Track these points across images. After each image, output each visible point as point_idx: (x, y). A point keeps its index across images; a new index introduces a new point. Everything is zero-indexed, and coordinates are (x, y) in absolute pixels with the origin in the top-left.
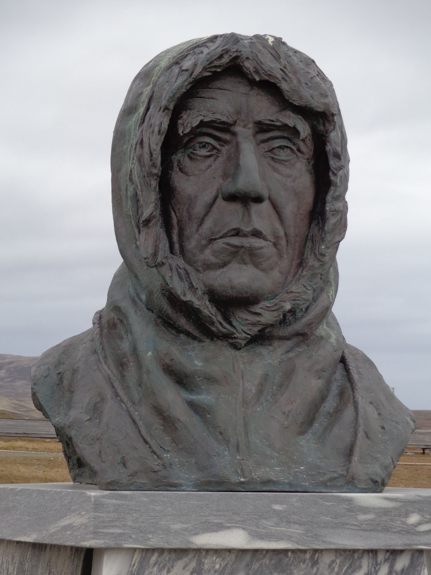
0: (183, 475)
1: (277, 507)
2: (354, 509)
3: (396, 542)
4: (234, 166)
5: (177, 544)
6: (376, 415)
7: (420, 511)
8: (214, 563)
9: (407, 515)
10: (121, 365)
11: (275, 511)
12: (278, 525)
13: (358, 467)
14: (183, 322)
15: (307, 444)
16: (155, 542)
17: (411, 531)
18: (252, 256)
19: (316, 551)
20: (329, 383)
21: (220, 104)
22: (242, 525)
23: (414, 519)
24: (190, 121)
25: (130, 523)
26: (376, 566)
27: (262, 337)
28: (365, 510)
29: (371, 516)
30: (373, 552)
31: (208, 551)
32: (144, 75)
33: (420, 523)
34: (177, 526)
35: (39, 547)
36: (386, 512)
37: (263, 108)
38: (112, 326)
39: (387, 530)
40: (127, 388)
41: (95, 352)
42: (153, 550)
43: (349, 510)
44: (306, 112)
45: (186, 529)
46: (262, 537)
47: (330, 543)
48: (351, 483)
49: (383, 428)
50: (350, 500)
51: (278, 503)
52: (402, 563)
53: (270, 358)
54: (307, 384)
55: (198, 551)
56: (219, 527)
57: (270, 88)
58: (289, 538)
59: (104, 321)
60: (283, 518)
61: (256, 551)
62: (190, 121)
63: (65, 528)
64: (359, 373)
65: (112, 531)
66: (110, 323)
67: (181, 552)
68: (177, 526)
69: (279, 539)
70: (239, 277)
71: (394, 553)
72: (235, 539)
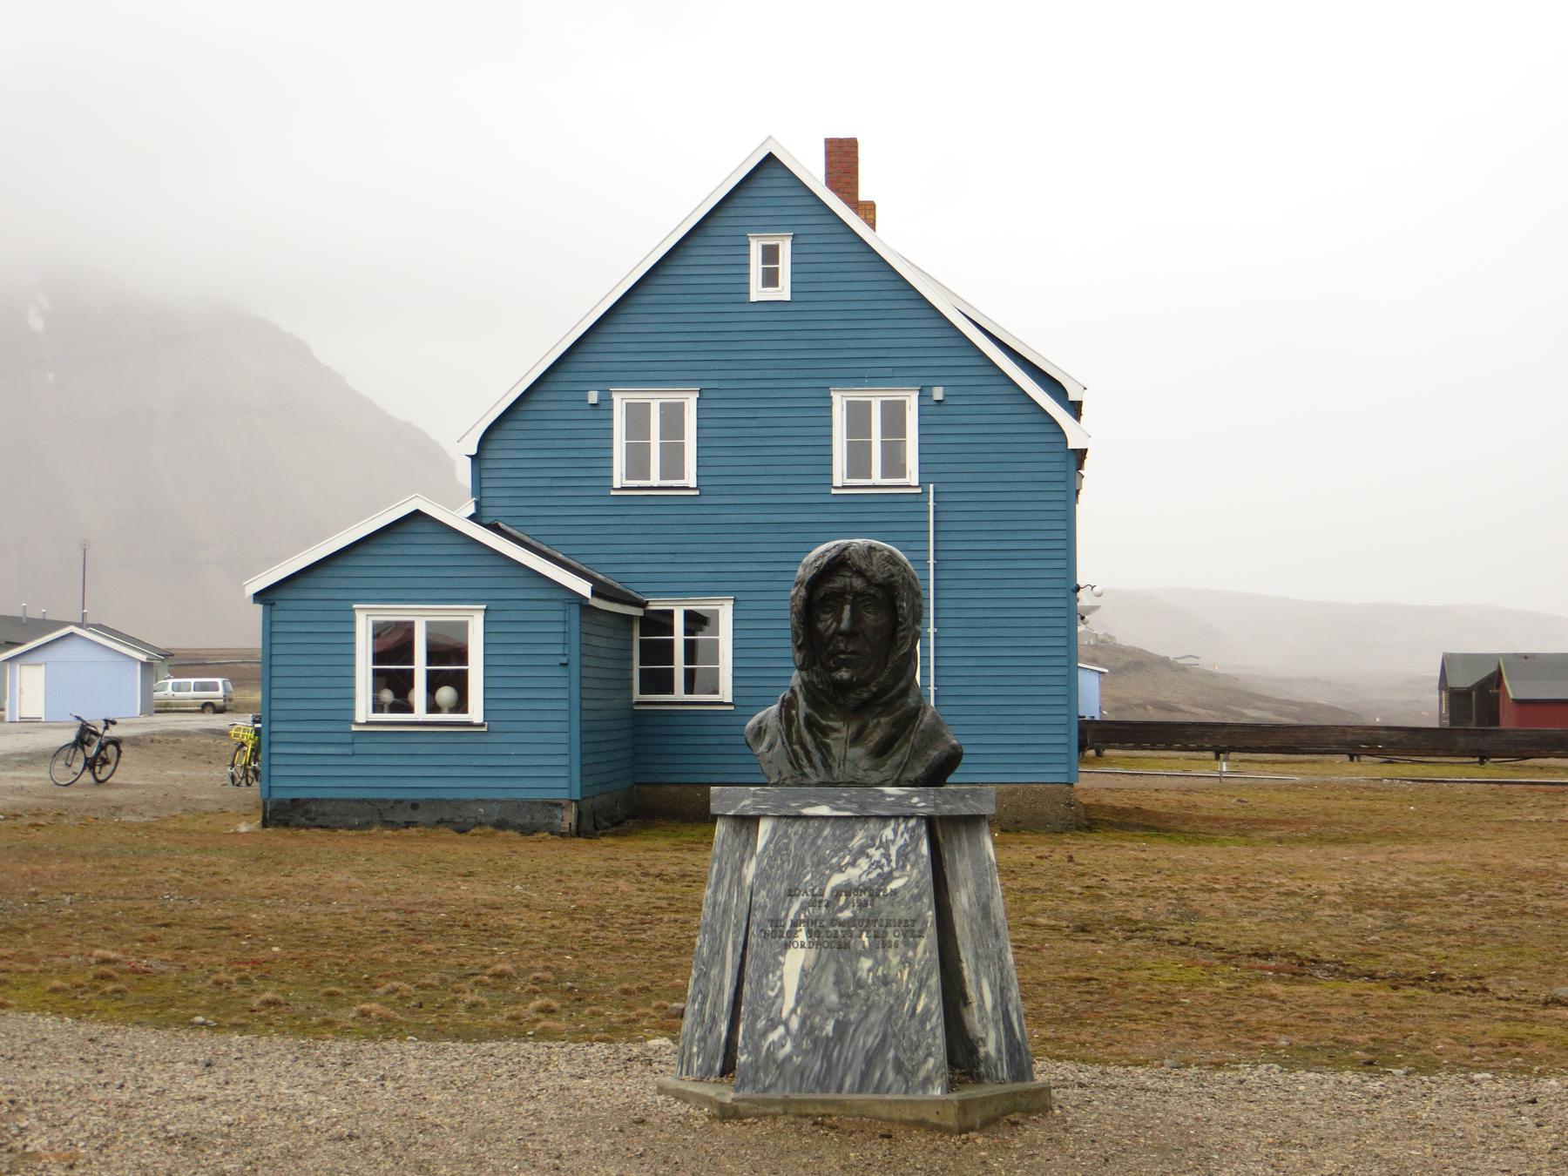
2: (884, 795)
3: (908, 812)
17: (914, 806)
22: (827, 803)
23: (915, 800)
30: (896, 817)
52: (912, 823)
60: (849, 801)
61: (837, 817)
72: (824, 810)
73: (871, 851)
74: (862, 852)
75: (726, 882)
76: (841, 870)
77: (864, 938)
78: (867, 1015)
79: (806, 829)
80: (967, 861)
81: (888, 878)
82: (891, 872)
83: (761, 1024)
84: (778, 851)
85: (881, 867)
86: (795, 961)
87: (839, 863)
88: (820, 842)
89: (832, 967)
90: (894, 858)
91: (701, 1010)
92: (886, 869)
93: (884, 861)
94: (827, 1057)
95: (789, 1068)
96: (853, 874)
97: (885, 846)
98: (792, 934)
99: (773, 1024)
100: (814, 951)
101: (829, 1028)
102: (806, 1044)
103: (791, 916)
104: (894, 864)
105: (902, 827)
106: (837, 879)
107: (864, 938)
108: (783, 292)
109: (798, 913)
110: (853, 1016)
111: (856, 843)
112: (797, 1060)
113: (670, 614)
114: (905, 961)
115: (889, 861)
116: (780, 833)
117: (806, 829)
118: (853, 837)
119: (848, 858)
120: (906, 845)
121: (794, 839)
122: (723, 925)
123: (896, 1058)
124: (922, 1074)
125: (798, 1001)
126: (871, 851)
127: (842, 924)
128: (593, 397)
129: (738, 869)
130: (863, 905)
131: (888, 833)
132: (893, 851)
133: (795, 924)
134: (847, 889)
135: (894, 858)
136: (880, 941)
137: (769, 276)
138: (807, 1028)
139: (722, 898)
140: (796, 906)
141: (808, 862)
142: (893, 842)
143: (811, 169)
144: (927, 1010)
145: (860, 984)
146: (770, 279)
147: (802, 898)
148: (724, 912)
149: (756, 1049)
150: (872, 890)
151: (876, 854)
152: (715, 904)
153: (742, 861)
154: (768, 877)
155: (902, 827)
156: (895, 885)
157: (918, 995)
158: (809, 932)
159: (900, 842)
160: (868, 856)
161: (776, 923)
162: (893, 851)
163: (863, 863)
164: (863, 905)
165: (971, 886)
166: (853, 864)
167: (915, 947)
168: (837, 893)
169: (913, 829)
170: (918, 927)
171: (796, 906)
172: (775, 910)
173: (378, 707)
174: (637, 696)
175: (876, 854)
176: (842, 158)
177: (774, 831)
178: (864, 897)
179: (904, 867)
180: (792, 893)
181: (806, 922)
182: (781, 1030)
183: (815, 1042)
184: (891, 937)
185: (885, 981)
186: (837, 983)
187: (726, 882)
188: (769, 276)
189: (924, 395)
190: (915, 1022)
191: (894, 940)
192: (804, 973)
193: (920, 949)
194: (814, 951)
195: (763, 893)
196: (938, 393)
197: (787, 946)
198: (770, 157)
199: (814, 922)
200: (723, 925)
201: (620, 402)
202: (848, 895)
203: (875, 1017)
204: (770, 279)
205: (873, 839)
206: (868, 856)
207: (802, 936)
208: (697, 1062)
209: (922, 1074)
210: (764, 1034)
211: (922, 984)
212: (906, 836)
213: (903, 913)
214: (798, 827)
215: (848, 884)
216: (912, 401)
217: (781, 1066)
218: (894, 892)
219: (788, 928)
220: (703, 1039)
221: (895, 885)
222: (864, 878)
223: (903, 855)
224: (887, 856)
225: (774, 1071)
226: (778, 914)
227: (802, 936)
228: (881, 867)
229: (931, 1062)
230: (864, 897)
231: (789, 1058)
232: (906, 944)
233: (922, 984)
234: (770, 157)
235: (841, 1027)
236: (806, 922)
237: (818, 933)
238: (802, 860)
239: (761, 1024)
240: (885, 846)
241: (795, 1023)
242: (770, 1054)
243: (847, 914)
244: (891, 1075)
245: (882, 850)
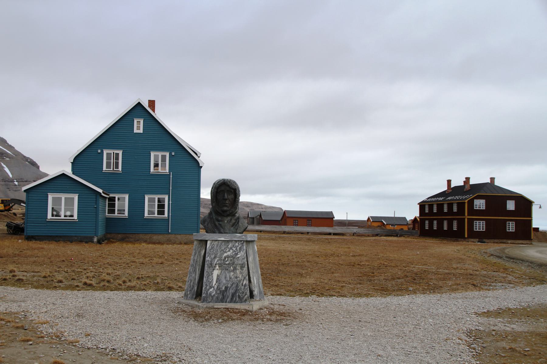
0: (217, 232)
4: (224, 196)
10: (211, 219)
13: (238, 231)
15: (232, 228)
18: (226, 206)
21: (223, 188)
24: (219, 190)
27: (228, 216)
32: (214, 184)
35: (201, 240)
37: (228, 188)
44: (233, 189)
48: (236, 233)
51: (228, 235)
53: (229, 218)
54: (233, 221)
57: (228, 186)
62: (219, 190)
66: (210, 214)
70: (225, 208)
71: (241, 241)
72: (223, 239)
74: (231, 248)
76: (226, 252)
78: (232, 285)
81: (237, 254)
83: (208, 287)
84: (212, 248)
86: (216, 273)
89: (224, 274)
91: (190, 284)
94: (223, 295)
95: (215, 298)
96: (229, 253)
97: (236, 247)
98: (215, 267)
99: (211, 287)
100: (220, 271)
101: (224, 288)
102: (218, 292)
106: (225, 254)
108: (141, 131)
110: (229, 285)
111: (229, 246)
112: (216, 295)
113: (115, 197)
114: (241, 273)
123: (239, 295)
124: (244, 299)
125: (217, 282)
128: (99, 151)
129: (200, 252)
130: (231, 260)
131: (237, 244)
132: (238, 248)
133: (216, 264)
134: (228, 257)
136: (235, 269)
138: (218, 288)
139: (196, 258)
140: (216, 261)
143: (146, 105)
144: (245, 284)
145: (230, 278)
146: (138, 128)
149: (207, 293)
150: (233, 257)
151: (234, 249)
152: (194, 260)
156: (238, 256)
157: (243, 281)
161: (211, 264)
162: (238, 248)
163: (231, 251)
164: (231, 260)
166: (229, 251)
168: (225, 258)
171: (216, 261)
172: (211, 261)
173: (53, 215)
174: (107, 214)
175: (234, 249)
176: (152, 104)
177: (211, 243)
180: (215, 258)
182: (213, 289)
183: (220, 291)
184: (237, 268)
185: (236, 278)
186: (225, 278)
189: (170, 154)
190: (243, 287)
192: (218, 276)
196: (173, 154)
197: (214, 269)
198: (139, 103)
201: (105, 152)
203: (234, 286)
204: (138, 128)
207: (217, 267)
208: (189, 296)
209: (244, 299)
210: (209, 290)
211: (245, 278)
213: (240, 262)
214: (216, 242)
216: (167, 154)
217: (213, 297)
220: (191, 291)
221: (238, 256)
223: (240, 249)
224: (236, 249)
225: (211, 298)
227: (217, 267)
229: (246, 296)
231: (214, 295)
233: (245, 278)
235: (226, 288)
239: (208, 287)
240: (236, 247)
241: (216, 287)
242: (210, 294)
243: (227, 262)
244: (238, 299)
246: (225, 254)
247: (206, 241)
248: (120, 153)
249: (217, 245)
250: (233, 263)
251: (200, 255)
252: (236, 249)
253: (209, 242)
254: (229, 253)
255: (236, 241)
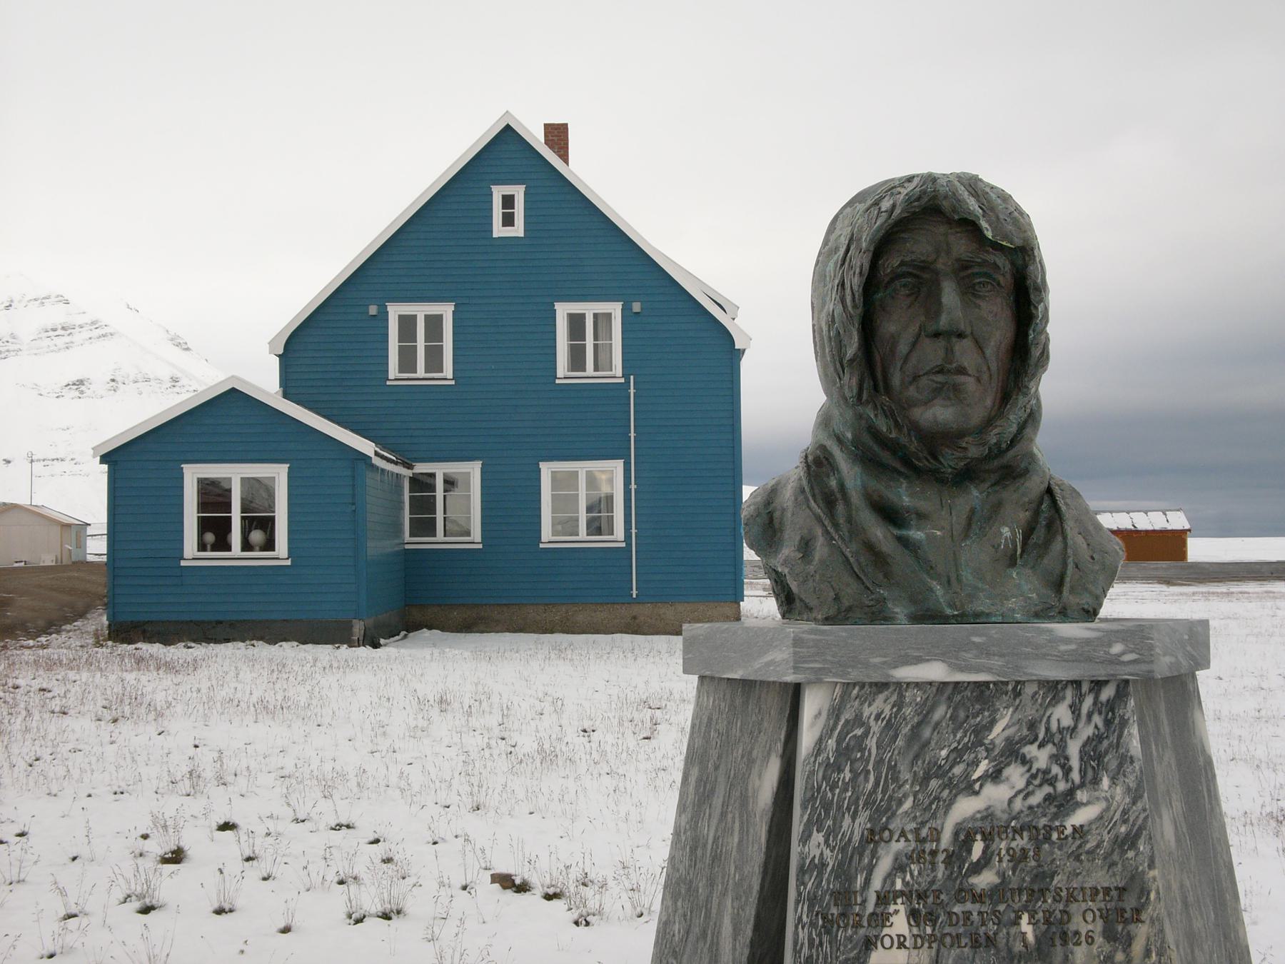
1: (976, 639)
2: (1057, 640)
3: (1101, 673)
5: (877, 677)
6: (1085, 546)
7: (1124, 640)
8: (915, 695)
9: (1110, 646)
11: (974, 643)
12: (977, 657)
14: (886, 457)
16: (854, 675)
17: (1115, 661)
19: (1018, 682)
20: (1037, 512)
23: (1117, 648)
25: (829, 658)
26: (1081, 698)
28: (1068, 641)
29: (1073, 647)
30: (1077, 684)
31: (908, 684)
33: (1123, 653)
34: (877, 660)
35: (747, 686)
36: (1088, 642)
38: (818, 462)
39: (1089, 659)
40: (836, 526)
41: (803, 491)
42: (855, 685)
43: (1050, 641)
45: (884, 663)
46: (961, 669)
47: (1032, 675)
49: (1092, 558)
50: (1050, 631)
55: (899, 684)
56: (918, 660)
58: (989, 670)
59: (810, 458)
60: (983, 650)
61: (957, 684)
63: (768, 664)
64: (1066, 504)
65: (811, 665)
67: (881, 686)
68: (877, 660)
69: (978, 670)
71: (1098, 685)
72: (935, 671)
73: (1031, 750)
74: (1012, 752)
75: (718, 801)
76: (970, 789)
77: (1026, 926)
79: (899, 705)
80: (1169, 756)
81: (1065, 803)
82: (1071, 792)
84: (844, 753)
85: (1052, 782)
87: (967, 774)
88: (927, 733)
90: (1075, 763)
92: (1062, 786)
93: (1056, 770)
96: (995, 795)
98: (881, 919)
103: (877, 884)
104: (1075, 776)
105: (1088, 702)
106: (966, 807)
107: (1026, 926)
109: (890, 877)
111: (998, 733)
115: (1067, 771)
116: (847, 715)
117: (899, 705)
118: (993, 722)
119: (984, 766)
120: (1098, 738)
121: (876, 728)
122: (711, 883)
126: (1031, 750)
127: (978, 898)
128: (373, 310)
130: (1018, 858)
131: (1061, 714)
132: (1074, 749)
134: (988, 827)
135: (1075, 763)
137: (508, 217)
140: (885, 864)
141: (906, 775)
142: (1073, 730)
143: (536, 137)
147: (898, 846)
148: (716, 858)
150: (1039, 826)
151: (1041, 757)
153: (751, 762)
154: (827, 806)
155: (1088, 702)
156: (1081, 817)
158: (913, 915)
159: (1086, 732)
160: (1024, 761)
161: (844, 896)
162: (1074, 749)
163: (1016, 775)
165: (1178, 805)
166: (995, 776)
167: (1128, 941)
168: (964, 838)
169: (1111, 706)
170: (1130, 903)
171: (885, 864)
172: (844, 872)
173: (202, 547)
174: (407, 538)
175: (1041, 757)
178: (1021, 842)
179: (1096, 781)
180: (874, 837)
181: (906, 895)
187: (718, 801)
188: (508, 217)
191: (1083, 929)
193: (1138, 948)
194: (925, 955)
195: (818, 837)
199: (922, 896)
200: (711, 883)
201: (395, 311)
202: (987, 838)
205: (1032, 726)
206: (1024, 761)
207: (899, 924)
212: (1097, 719)
213: (1100, 878)
215: (988, 814)
218: (1079, 831)
219: (870, 908)
221: (1081, 817)
222: (1018, 804)
223: (1094, 755)
224: (1061, 758)
226: (851, 879)
227: (899, 924)
228: (1052, 782)
230: (1021, 842)
232: (1109, 935)
234: (508, 128)
236: (906, 895)
237: (932, 918)
238: (893, 768)
243: (985, 880)
245: (1050, 749)
246: (966, 807)
247: (795, 694)
248: (446, 311)
249: (891, 727)
250: (1039, 886)
251: (744, 800)
252: (1061, 758)
253: (813, 705)
254: (995, 795)
255: (1053, 689)
